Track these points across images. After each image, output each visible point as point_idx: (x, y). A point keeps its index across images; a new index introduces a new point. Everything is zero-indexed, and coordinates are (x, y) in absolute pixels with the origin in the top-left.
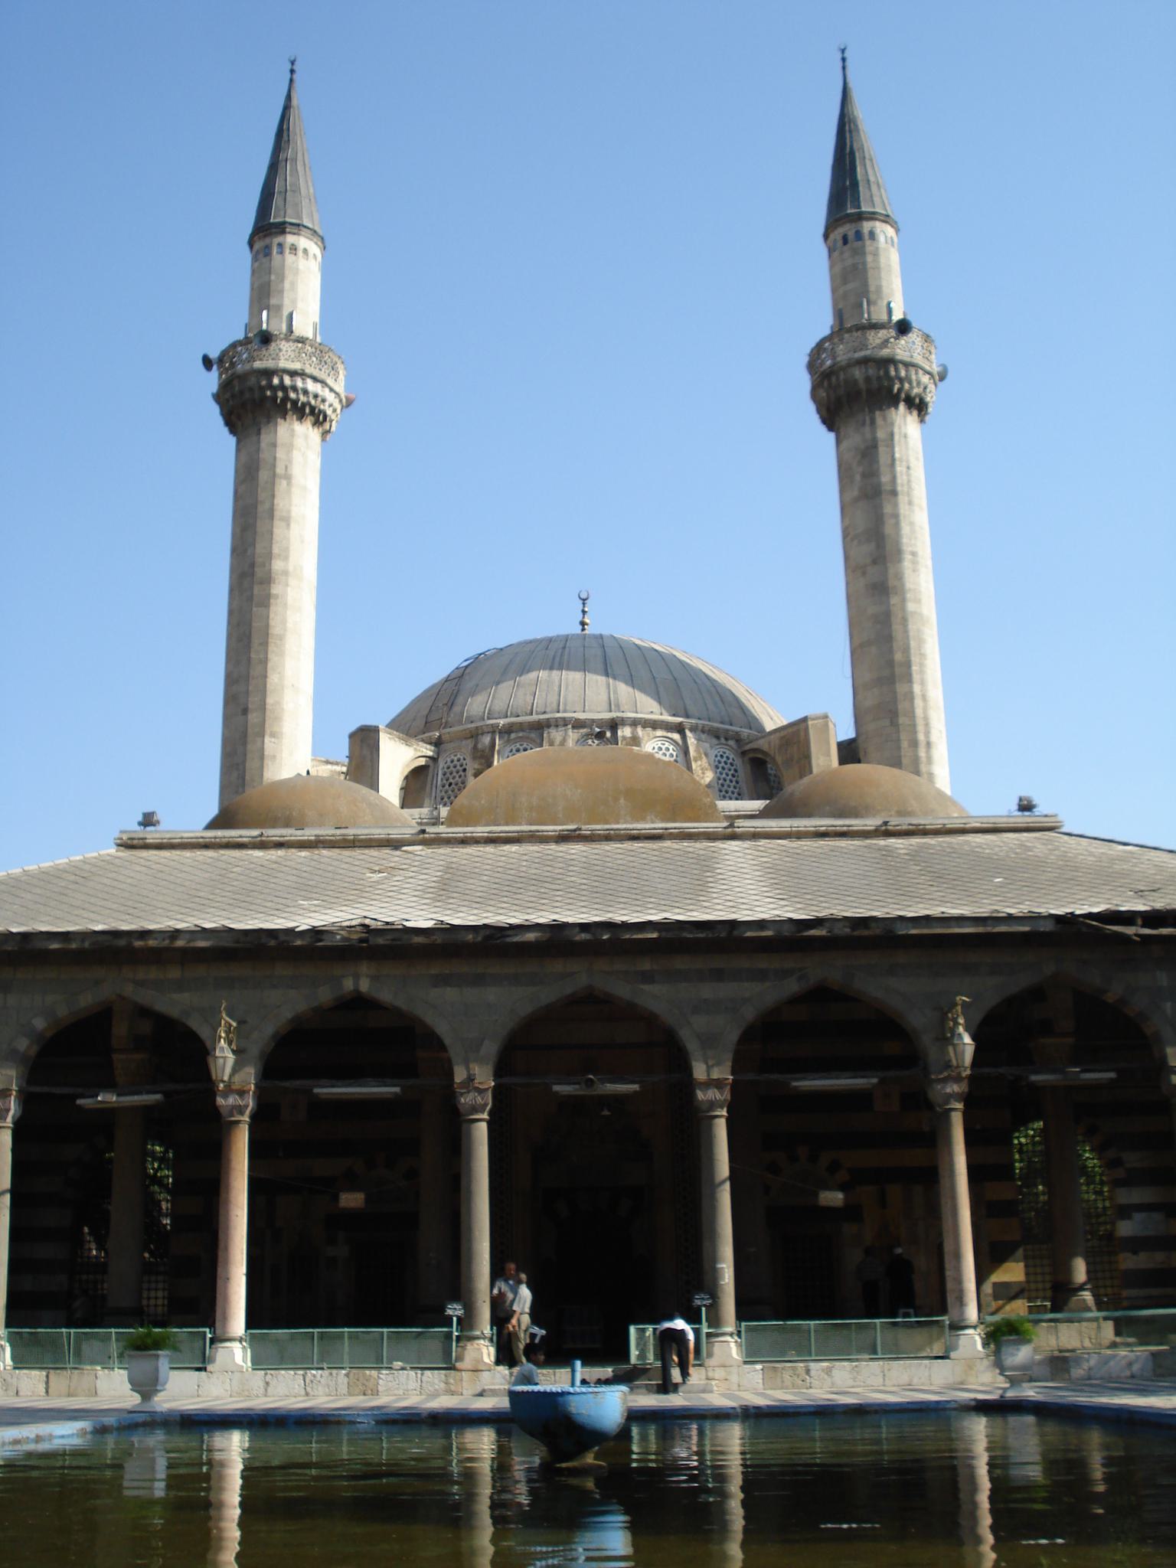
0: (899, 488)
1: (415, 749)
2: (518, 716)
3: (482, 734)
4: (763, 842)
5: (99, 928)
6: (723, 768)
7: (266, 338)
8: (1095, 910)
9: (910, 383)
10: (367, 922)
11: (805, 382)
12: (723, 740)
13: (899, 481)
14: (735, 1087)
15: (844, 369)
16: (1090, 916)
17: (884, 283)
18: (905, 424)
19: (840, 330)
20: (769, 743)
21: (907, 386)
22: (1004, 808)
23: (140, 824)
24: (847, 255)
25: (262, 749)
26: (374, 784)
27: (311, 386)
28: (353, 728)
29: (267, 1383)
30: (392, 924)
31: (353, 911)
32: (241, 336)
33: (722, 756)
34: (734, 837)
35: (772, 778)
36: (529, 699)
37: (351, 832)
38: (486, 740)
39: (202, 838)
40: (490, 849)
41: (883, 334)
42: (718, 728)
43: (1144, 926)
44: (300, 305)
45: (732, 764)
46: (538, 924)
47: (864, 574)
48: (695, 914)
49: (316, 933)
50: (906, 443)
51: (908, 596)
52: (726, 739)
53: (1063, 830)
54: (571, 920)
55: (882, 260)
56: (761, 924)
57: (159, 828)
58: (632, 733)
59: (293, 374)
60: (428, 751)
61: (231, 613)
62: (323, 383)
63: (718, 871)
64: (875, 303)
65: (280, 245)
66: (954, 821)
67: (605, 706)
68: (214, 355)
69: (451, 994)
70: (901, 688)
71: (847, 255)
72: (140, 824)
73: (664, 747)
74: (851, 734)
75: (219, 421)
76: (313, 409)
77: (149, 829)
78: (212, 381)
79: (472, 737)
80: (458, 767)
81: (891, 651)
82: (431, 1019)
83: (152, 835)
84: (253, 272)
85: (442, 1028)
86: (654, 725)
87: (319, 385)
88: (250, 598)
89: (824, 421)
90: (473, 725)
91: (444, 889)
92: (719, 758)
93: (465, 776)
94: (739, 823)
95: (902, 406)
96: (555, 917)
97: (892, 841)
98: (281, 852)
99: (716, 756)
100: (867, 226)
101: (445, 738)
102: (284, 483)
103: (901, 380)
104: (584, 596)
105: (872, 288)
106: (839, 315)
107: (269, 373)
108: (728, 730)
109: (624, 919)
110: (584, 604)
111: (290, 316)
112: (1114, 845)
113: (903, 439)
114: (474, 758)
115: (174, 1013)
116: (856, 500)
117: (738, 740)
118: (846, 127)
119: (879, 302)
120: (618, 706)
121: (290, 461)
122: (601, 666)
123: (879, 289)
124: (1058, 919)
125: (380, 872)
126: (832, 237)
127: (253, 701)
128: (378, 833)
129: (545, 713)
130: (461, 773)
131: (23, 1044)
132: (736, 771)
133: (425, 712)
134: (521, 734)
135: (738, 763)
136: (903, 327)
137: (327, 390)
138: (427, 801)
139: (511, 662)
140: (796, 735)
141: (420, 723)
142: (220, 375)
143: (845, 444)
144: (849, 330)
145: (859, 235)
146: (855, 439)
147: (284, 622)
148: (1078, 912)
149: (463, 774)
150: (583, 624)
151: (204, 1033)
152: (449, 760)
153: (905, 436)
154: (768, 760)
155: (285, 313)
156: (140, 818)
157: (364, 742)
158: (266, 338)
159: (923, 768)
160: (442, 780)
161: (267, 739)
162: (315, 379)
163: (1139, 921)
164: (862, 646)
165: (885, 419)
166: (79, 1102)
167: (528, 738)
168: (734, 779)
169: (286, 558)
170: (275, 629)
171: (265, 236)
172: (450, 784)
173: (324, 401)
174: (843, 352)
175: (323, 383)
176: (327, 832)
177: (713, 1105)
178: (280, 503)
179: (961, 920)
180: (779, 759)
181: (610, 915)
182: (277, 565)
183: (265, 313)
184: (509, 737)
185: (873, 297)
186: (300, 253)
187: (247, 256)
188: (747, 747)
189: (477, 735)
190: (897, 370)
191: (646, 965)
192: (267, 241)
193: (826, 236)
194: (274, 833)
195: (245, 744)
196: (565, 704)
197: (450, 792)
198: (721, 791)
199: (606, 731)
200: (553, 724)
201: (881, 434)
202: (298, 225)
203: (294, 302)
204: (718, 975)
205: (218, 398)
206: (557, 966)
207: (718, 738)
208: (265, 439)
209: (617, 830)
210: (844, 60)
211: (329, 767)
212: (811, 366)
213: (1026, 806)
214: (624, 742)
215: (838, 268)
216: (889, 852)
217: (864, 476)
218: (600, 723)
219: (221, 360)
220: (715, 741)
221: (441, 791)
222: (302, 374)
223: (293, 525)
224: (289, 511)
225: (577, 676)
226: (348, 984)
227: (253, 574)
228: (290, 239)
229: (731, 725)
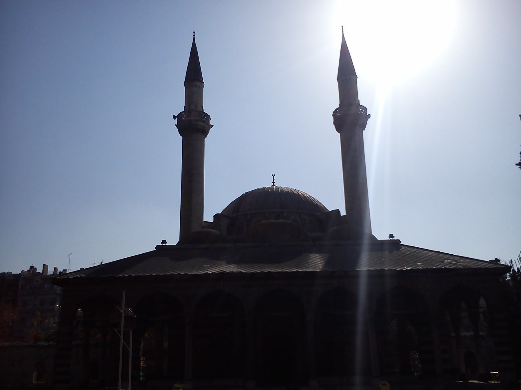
10: (222, 272)
11: (332, 119)
23: (162, 243)
27: (201, 124)
31: (219, 268)
68: (176, 115)
72: (162, 243)
74: (345, 214)
78: (176, 121)
89: (337, 131)
104: (273, 175)
137: (206, 125)
213: (391, 236)
219: (177, 117)
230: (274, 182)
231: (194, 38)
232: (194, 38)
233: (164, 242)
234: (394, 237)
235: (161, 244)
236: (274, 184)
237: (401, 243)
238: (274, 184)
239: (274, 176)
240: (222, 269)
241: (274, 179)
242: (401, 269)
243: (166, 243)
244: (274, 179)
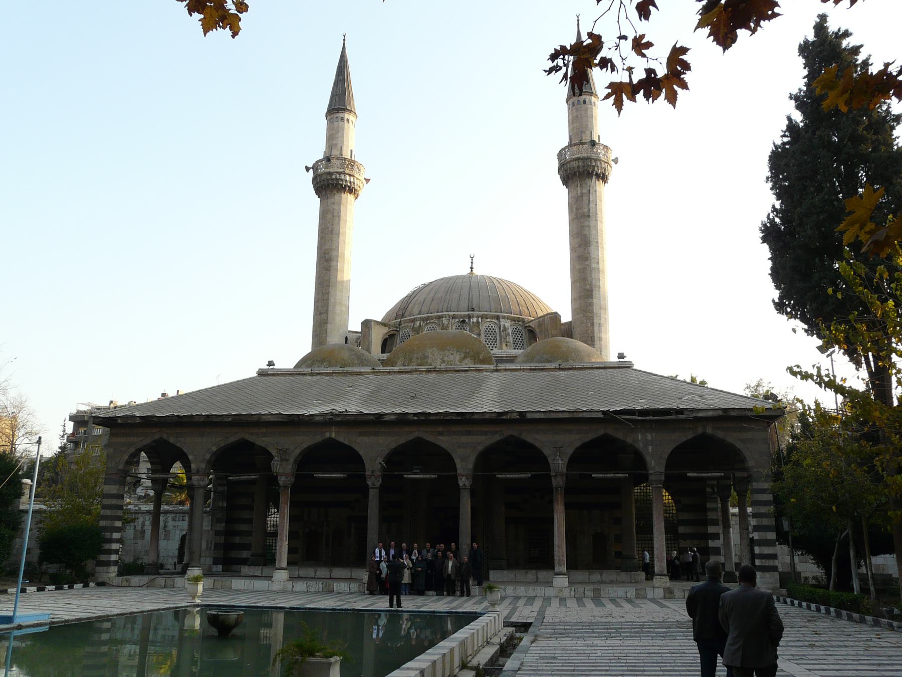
0: (591, 214)
10: (334, 411)
12: (517, 322)
13: (591, 211)
15: (568, 162)
16: (616, 412)
17: (589, 123)
18: (596, 186)
19: (571, 145)
21: (596, 169)
23: (267, 365)
27: (348, 178)
28: (363, 320)
29: (293, 586)
34: (497, 371)
37: (346, 369)
38: (418, 323)
40: (399, 376)
43: (638, 416)
50: (596, 194)
51: (593, 261)
54: (409, 411)
55: (589, 113)
59: (340, 173)
64: (585, 133)
68: (311, 166)
69: (366, 439)
72: (267, 365)
76: (349, 187)
82: (357, 448)
90: (413, 317)
95: (594, 179)
98: (318, 377)
102: (337, 219)
104: (472, 256)
113: (594, 193)
115: (263, 445)
117: (523, 320)
119: (587, 132)
124: (603, 412)
129: (442, 312)
131: (208, 456)
135: (523, 331)
139: (432, 289)
153: (596, 191)
155: (339, 147)
156: (267, 363)
159: (596, 335)
161: (328, 325)
162: (350, 175)
163: (637, 414)
165: (586, 184)
179: (563, 412)
182: (334, 253)
187: (324, 122)
188: (527, 325)
191: (440, 429)
192: (332, 116)
204: (469, 433)
206: (407, 429)
210: (578, 20)
213: (621, 356)
218: (465, 316)
226: (327, 435)
228: (341, 115)
230: (472, 268)
231: (344, 44)
232: (344, 44)
233: (271, 363)
234: (626, 357)
235: (267, 367)
236: (472, 271)
237: (634, 368)
238: (472, 271)
240: (334, 408)
241: (472, 263)
243: (274, 365)
244: (472, 263)
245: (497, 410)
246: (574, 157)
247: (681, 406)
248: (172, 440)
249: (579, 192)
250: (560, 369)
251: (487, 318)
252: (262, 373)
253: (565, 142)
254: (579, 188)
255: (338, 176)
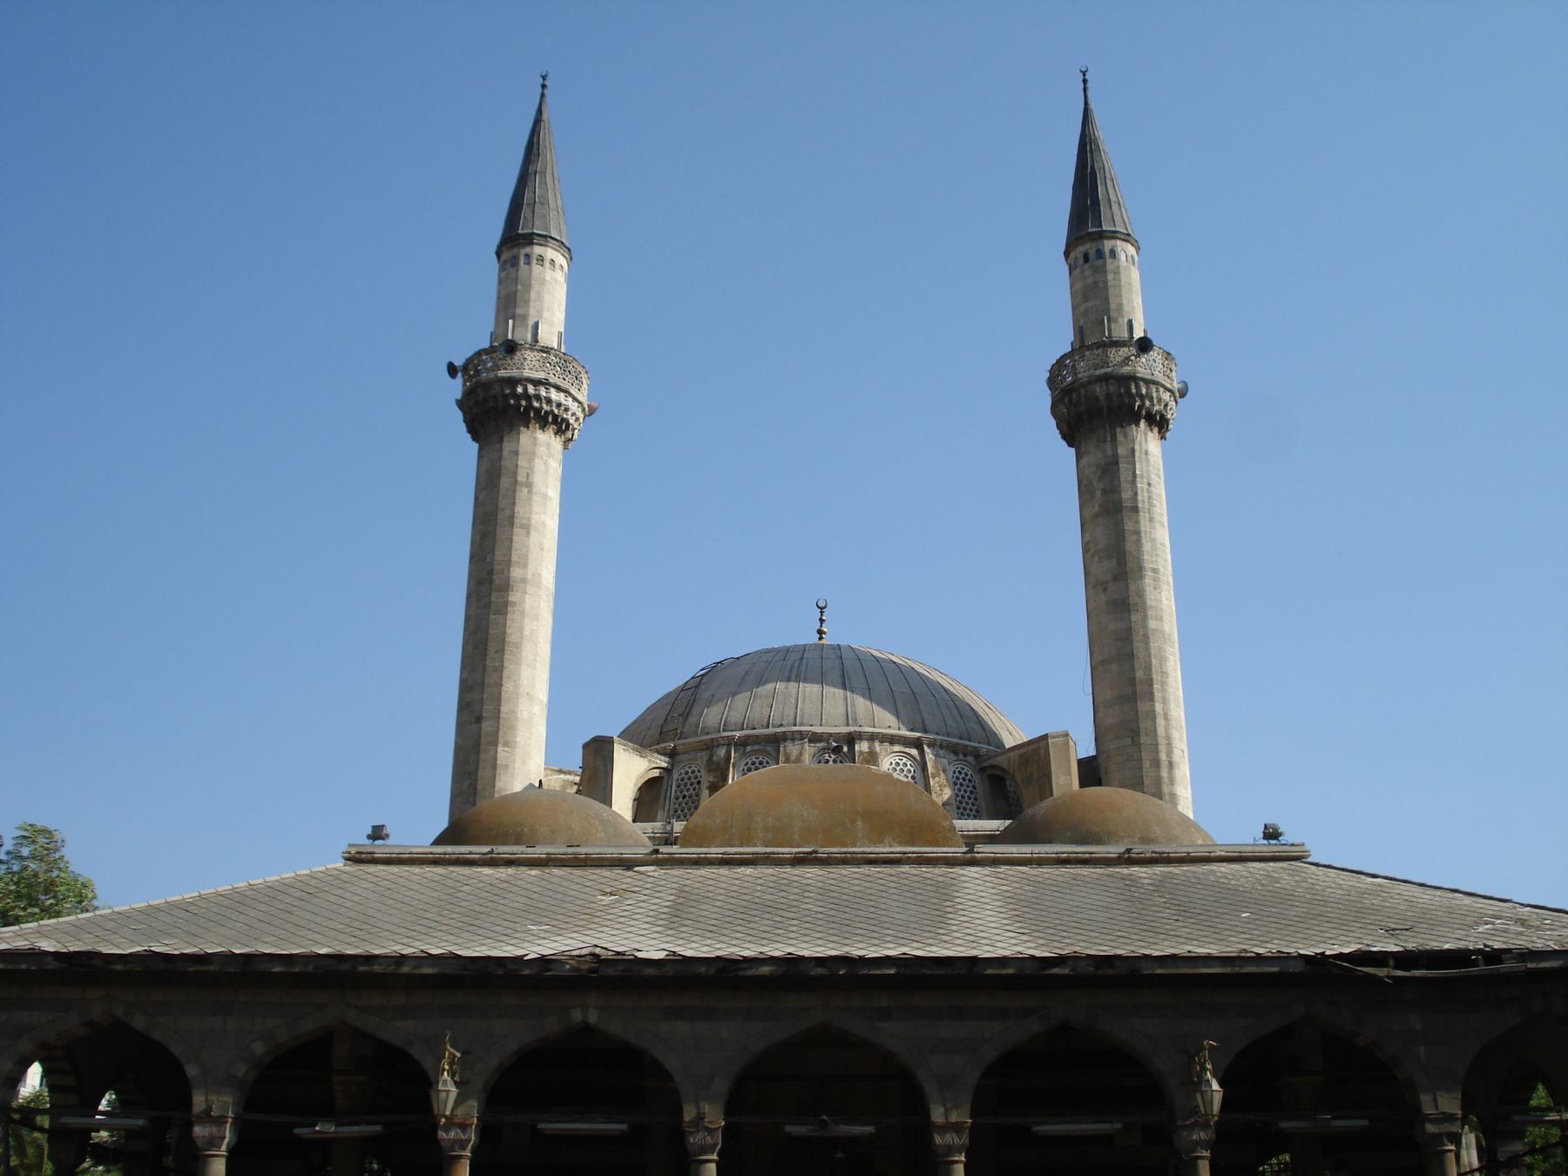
1: (650, 761)
2: (755, 729)
3: (718, 746)
4: (1003, 868)
5: (323, 951)
6: (961, 785)
7: (511, 348)
8: (1346, 951)
9: (1151, 399)
10: (597, 951)
12: (961, 756)
13: (1140, 498)
14: (975, 1131)
15: (1083, 385)
16: (1341, 956)
17: (1125, 301)
18: (1146, 441)
19: (1081, 346)
20: (1009, 759)
21: (1147, 403)
22: (1248, 836)
23: (369, 837)
24: (1088, 273)
25: (495, 759)
26: (606, 799)
27: (555, 395)
30: (623, 954)
31: (584, 938)
32: (486, 345)
33: (960, 772)
35: (1011, 795)
36: (766, 711)
38: (722, 752)
39: (432, 853)
40: (724, 871)
41: (1124, 351)
42: (957, 744)
43: (1396, 967)
44: (546, 315)
45: (970, 781)
46: (772, 958)
47: (1105, 590)
48: (934, 949)
49: (544, 961)
50: (1147, 459)
52: (965, 755)
53: (1309, 860)
54: (806, 953)
55: (1123, 279)
56: (1003, 961)
57: (388, 842)
58: (869, 748)
59: (537, 383)
60: (662, 762)
61: (468, 619)
62: (566, 392)
63: (958, 900)
64: (1116, 321)
65: (528, 256)
66: (1197, 847)
67: (843, 719)
68: (459, 362)
70: (1142, 707)
71: (1088, 273)
72: (369, 837)
73: (901, 763)
74: (1092, 752)
75: (463, 427)
76: (555, 417)
77: (377, 842)
78: (456, 387)
79: (707, 749)
80: (693, 780)
81: (1133, 669)
83: (381, 849)
84: (500, 282)
85: (672, 1063)
86: (892, 740)
87: (562, 395)
88: (488, 606)
89: (1064, 437)
90: (708, 737)
91: (677, 916)
92: (957, 774)
93: (700, 788)
94: (979, 848)
95: (1143, 423)
96: (790, 950)
97: (1136, 870)
98: (510, 871)
99: (954, 772)
100: (1107, 245)
101: (680, 749)
102: (525, 490)
103: (1142, 397)
105: (1113, 306)
106: (1080, 332)
107: (513, 382)
108: (967, 746)
109: (862, 953)
110: (822, 612)
111: (536, 326)
112: (1363, 877)
113: (1144, 456)
114: (709, 771)
116: (1097, 516)
117: (976, 754)
118: (1087, 147)
119: (1120, 319)
120: (855, 720)
121: (531, 468)
122: (840, 680)
123: (1120, 307)
124: (1307, 959)
125: (611, 894)
126: (1072, 255)
127: (488, 708)
128: (610, 851)
129: (781, 725)
130: (695, 785)
131: (241, 1070)
132: (974, 787)
133: (661, 722)
134: (756, 747)
135: (977, 779)
136: (1145, 345)
137: (570, 399)
138: (660, 815)
140: (1036, 753)
141: (655, 732)
142: (465, 382)
143: (1084, 462)
144: (1090, 348)
145: (1100, 254)
146: (1095, 456)
147: (521, 630)
148: (1328, 953)
149: (697, 787)
150: (820, 632)
151: (427, 1063)
152: (683, 771)
153: (1146, 453)
154: (1007, 777)
155: (531, 323)
156: (369, 831)
157: (598, 754)
158: (511, 348)
159: (1165, 789)
160: (676, 792)
161: (500, 749)
162: (558, 388)
163: (1391, 962)
164: (1103, 662)
165: (1126, 436)
166: (297, 1131)
167: (765, 751)
168: (972, 796)
169: (525, 566)
170: (512, 638)
171: (512, 247)
172: (684, 797)
173: (567, 410)
174: (1084, 369)
175: (566, 392)
176: (558, 850)
177: (951, 1150)
178: (520, 510)
179: (1208, 959)
180: (1019, 778)
181: (847, 949)
182: (516, 572)
183: (511, 322)
184: (745, 749)
185: (1113, 314)
186: (547, 264)
187: (493, 265)
188: (991, 762)
189: (713, 747)
190: (1138, 387)
192: (515, 251)
193: (1067, 254)
194: (504, 850)
195: (478, 753)
196: (802, 717)
197: (684, 805)
198: (959, 808)
199: (842, 746)
200: (789, 737)
201: (1121, 451)
202: (546, 237)
203: (540, 312)
205: (461, 404)
207: (956, 753)
208: (507, 447)
209: (854, 853)
210: (1085, 81)
211: (562, 776)
212: (1051, 382)
213: (1271, 834)
214: (861, 757)
215: (1079, 285)
216: (1132, 882)
217: (1104, 492)
218: (837, 737)
219: (465, 368)
220: (953, 757)
221: (675, 804)
222: (546, 383)
223: (532, 532)
224: (529, 519)
225: (816, 688)
226: (577, 1016)
227: (491, 582)
228: (537, 250)
229: (970, 740)
239: (822, 609)
242: (1319, 951)
245: (1037, 953)
246: (1097, 372)
247: (1497, 946)
248: (139, 1023)
249: (1109, 452)
250: (1127, 860)
251: (892, 743)
252: (357, 858)
253: (1063, 341)
254: (1108, 445)
255: (531, 389)
